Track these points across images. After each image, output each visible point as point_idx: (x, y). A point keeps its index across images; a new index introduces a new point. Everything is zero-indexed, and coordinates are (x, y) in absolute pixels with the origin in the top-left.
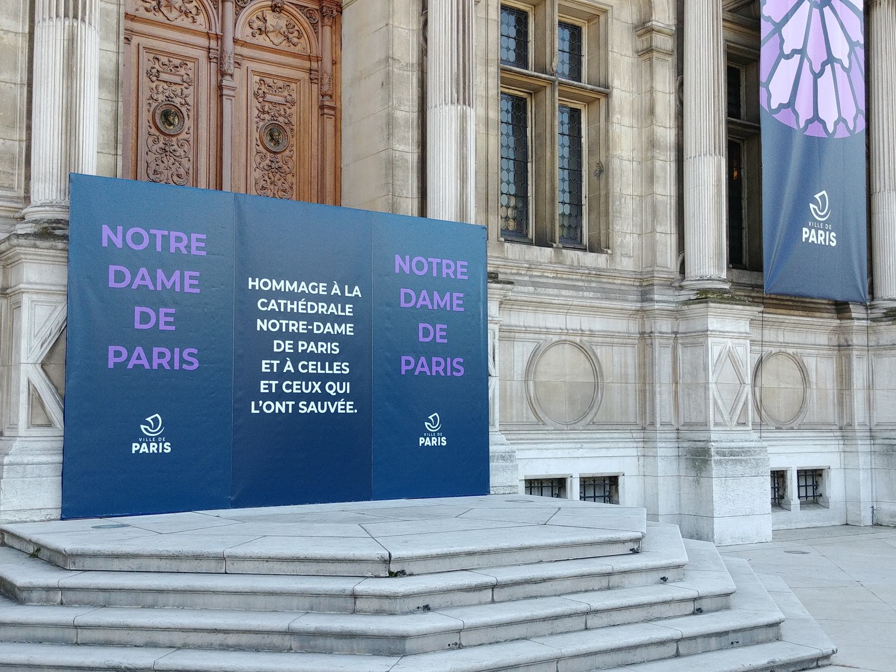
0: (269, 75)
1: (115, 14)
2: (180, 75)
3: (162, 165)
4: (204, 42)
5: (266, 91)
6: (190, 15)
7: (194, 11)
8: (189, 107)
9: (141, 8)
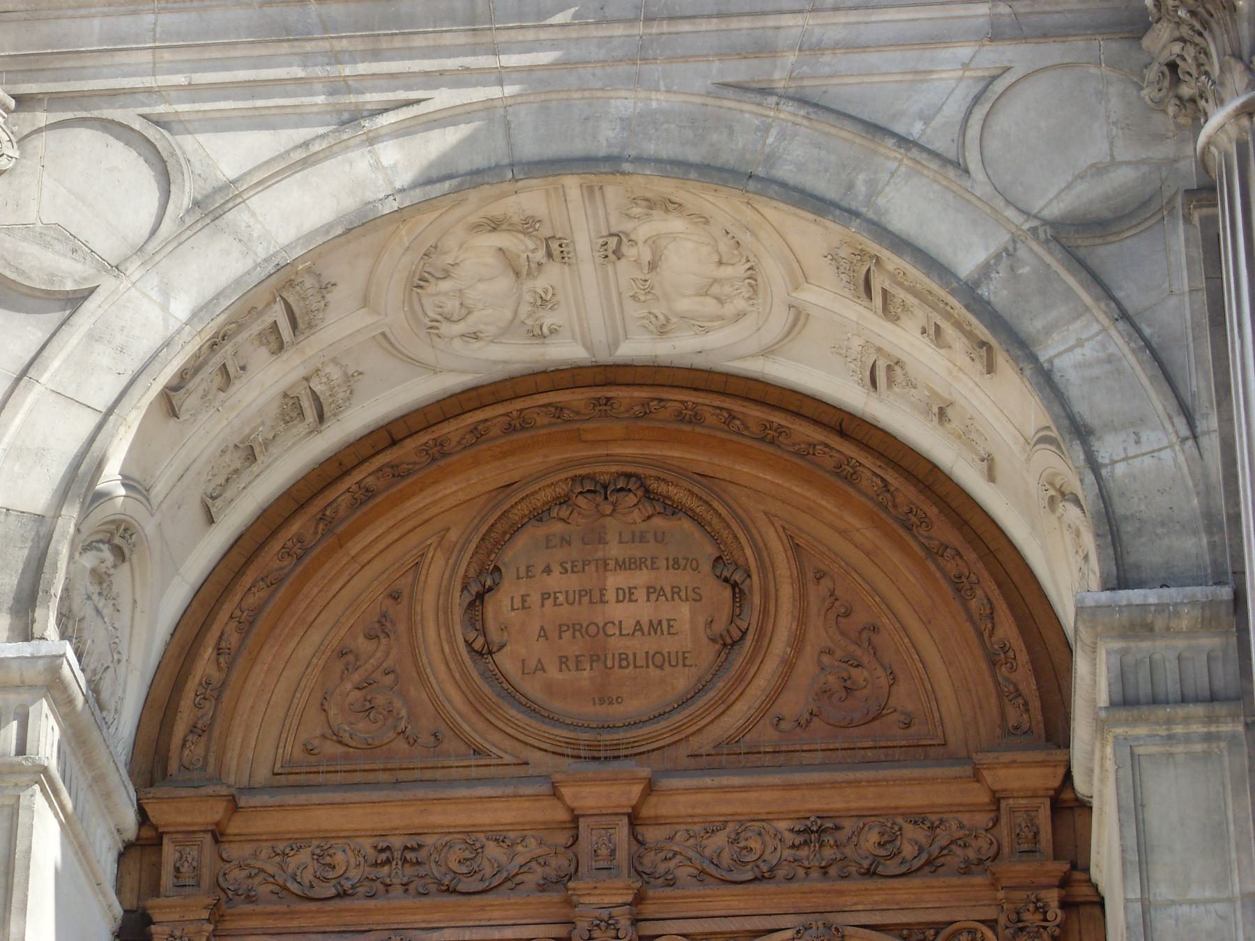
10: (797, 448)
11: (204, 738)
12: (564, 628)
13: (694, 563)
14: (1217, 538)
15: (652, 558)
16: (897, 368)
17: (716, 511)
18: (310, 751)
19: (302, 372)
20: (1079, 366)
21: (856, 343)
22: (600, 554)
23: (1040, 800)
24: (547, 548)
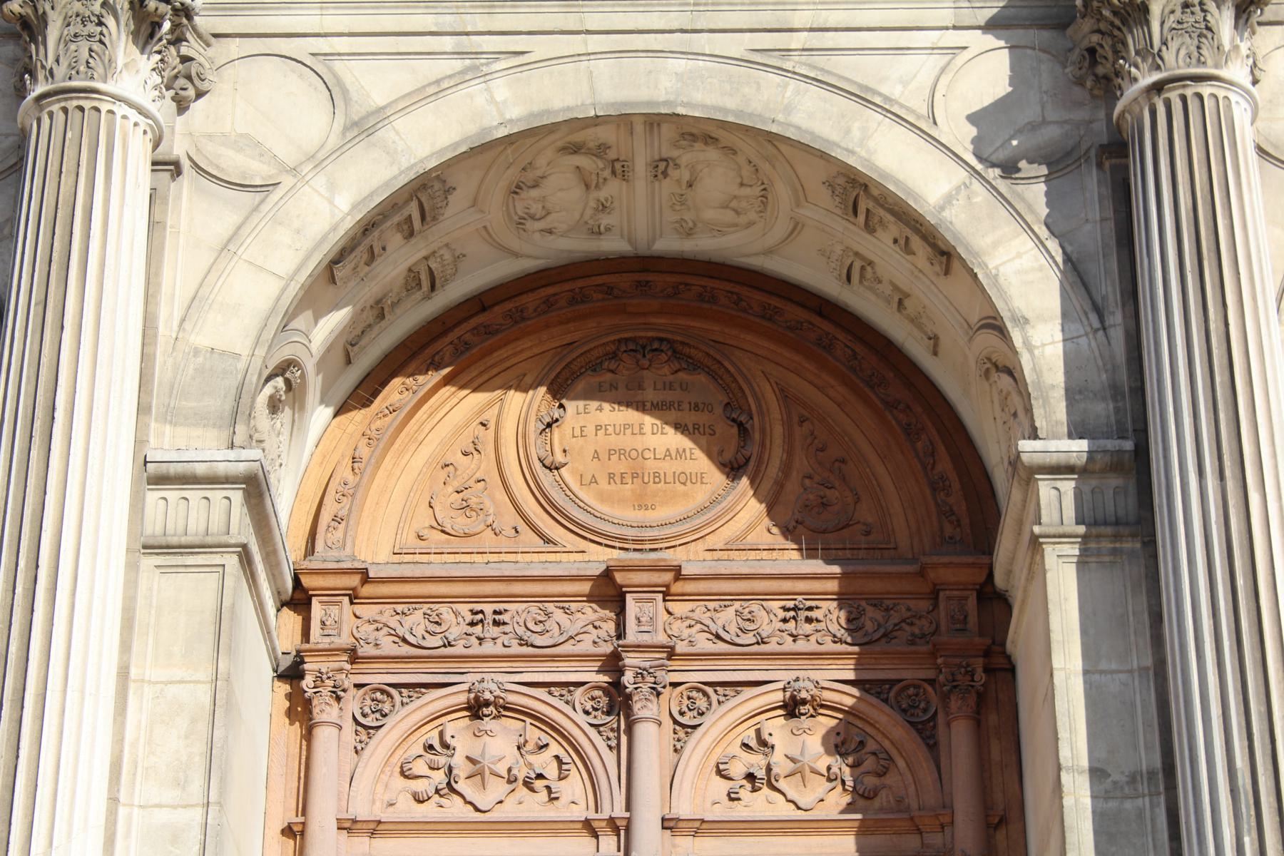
1: (196, 834)
7: (552, 771)
10: (789, 324)
11: (344, 523)
12: (613, 452)
13: (710, 407)
14: (1120, 404)
15: (679, 402)
16: (869, 269)
17: (726, 369)
18: (420, 537)
19: (424, 253)
21: (838, 249)
22: (639, 398)
23: (969, 592)
24: (600, 391)
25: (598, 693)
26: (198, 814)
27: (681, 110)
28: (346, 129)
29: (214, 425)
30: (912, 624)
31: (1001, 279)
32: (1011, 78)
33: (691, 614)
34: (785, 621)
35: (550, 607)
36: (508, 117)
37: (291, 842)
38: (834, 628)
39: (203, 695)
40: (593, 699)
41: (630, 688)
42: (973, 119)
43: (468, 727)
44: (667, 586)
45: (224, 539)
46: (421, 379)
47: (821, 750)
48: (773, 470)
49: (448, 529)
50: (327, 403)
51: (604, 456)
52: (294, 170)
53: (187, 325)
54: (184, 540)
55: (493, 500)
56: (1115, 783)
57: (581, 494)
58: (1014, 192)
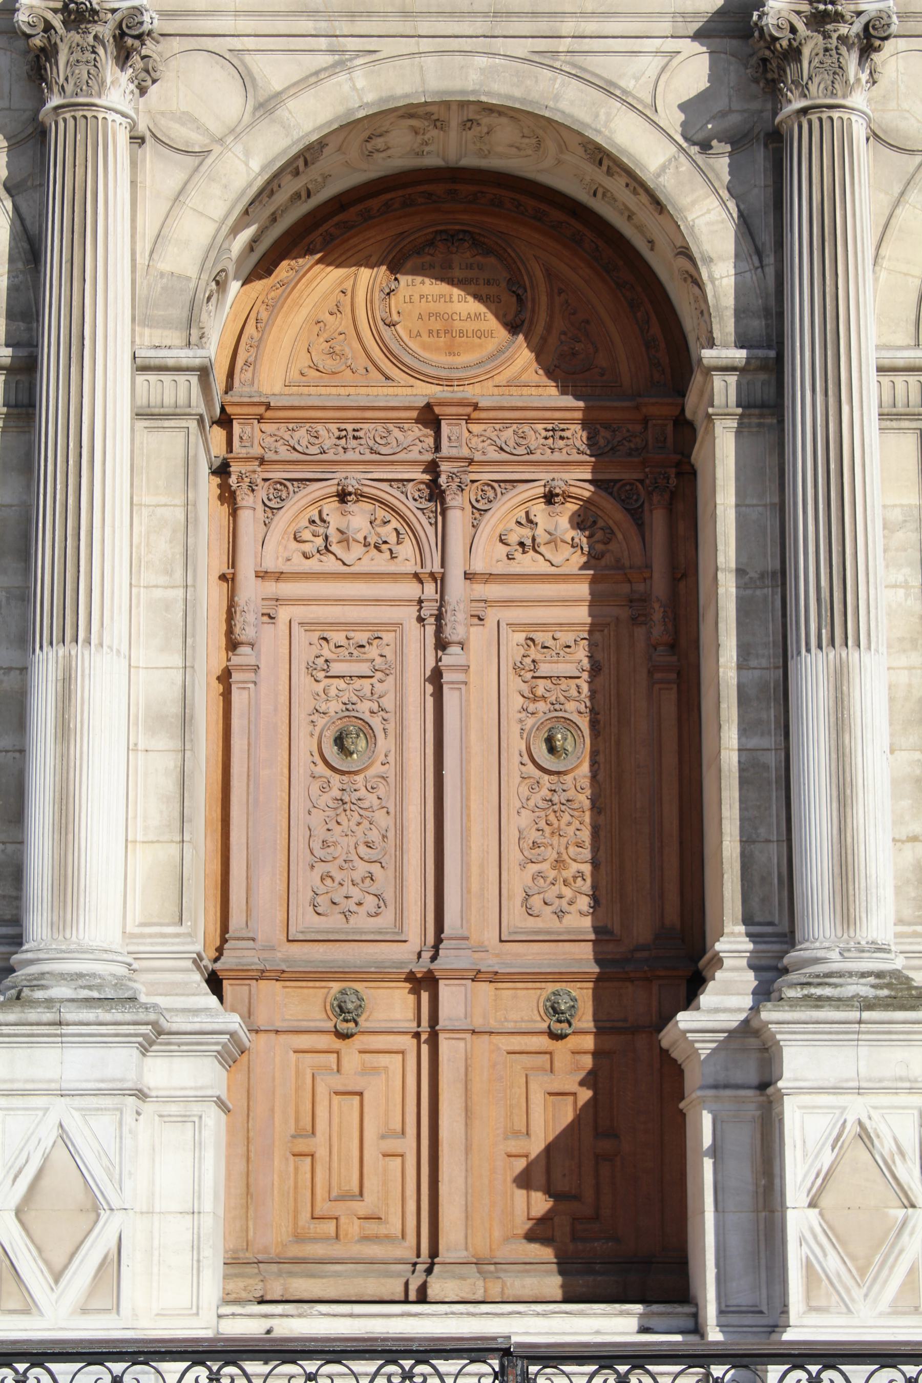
0: (543, 626)
1: (180, 605)
2: (367, 660)
3: (337, 830)
4: (412, 590)
5: (538, 657)
6: (384, 547)
7: (392, 539)
8: (386, 716)
9: (295, 555)
11: (252, 367)
14: (769, 322)
18: (302, 374)
20: (708, 224)
25: (422, 486)
26: (180, 592)
27: (484, 99)
28: (256, 109)
29: (176, 328)
30: (630, 441)
31: (696, 230)
32: (710, 76)
33: (483, 433)
34: (546, 438)
35: (391, 427)
36: (365, 101)
37: (226, 584)
38: (578, 443)
39: (180, 514)
40: (419, 490)
41: (444, 487)
42: (683, 107)
43: (338, 508)
44: (469, 416)
45: (188, 410)
46: (301, 261)
47: (568, 526)
48: (540, 328)
49: (321, 369)
50: (236, 278)
51: (426, 318)
52: (221, 141)
53: (155, 256)
54: (162, 411)
55: (351, 348)
56: (751, 578)
57: (411, 344)
58: (708, 165)
